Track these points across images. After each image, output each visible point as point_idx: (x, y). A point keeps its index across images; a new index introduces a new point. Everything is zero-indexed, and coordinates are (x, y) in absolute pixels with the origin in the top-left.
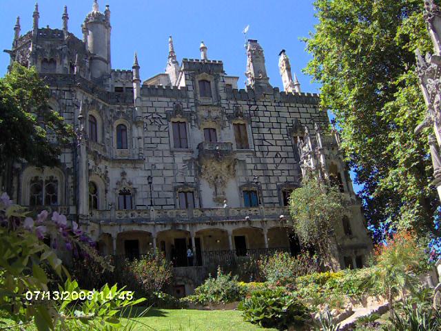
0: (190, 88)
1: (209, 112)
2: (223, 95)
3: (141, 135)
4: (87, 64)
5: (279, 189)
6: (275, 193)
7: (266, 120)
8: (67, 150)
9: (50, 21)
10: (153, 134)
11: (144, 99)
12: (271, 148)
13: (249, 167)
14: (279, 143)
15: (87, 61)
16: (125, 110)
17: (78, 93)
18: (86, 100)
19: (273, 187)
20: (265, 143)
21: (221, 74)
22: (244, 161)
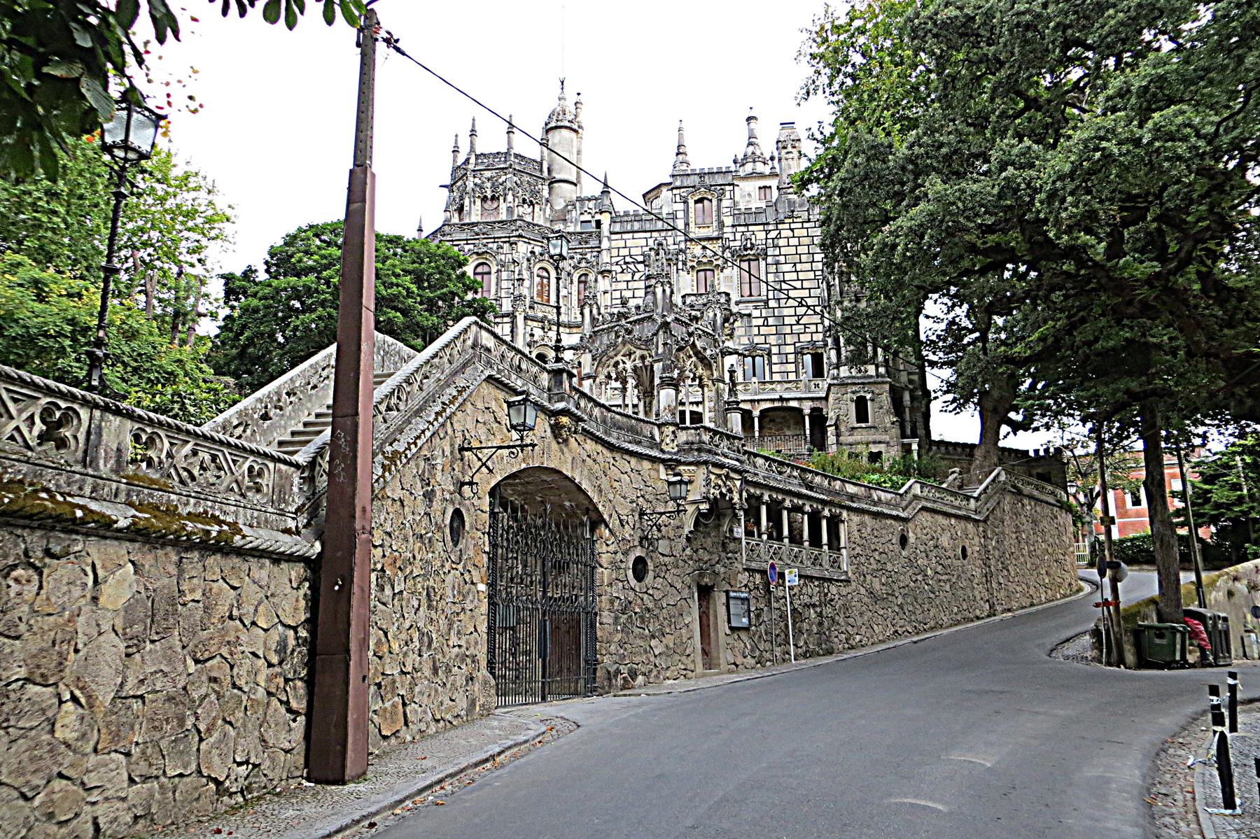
0: (680, 215)
1: (704, 248)
2: (728, 221)
3: (609, 288)
4: (545, 193)
5: (799, 352)
6: (791, 358)
7: (793, 250)
8: (506, 320)
9: (492, 140)
10: (624, 285)
11: (614, 237)
12: (792, 294)
13: (755, 322)
14: (806, 284)
15: (546, 187)
16: (588, 256)
17: (520, 244)
18: (532, 252)
19: (790, 349)
20: (784, 286)
21: (728, 188)
22: (749, 315)
